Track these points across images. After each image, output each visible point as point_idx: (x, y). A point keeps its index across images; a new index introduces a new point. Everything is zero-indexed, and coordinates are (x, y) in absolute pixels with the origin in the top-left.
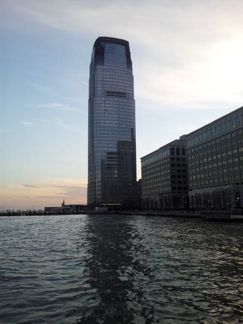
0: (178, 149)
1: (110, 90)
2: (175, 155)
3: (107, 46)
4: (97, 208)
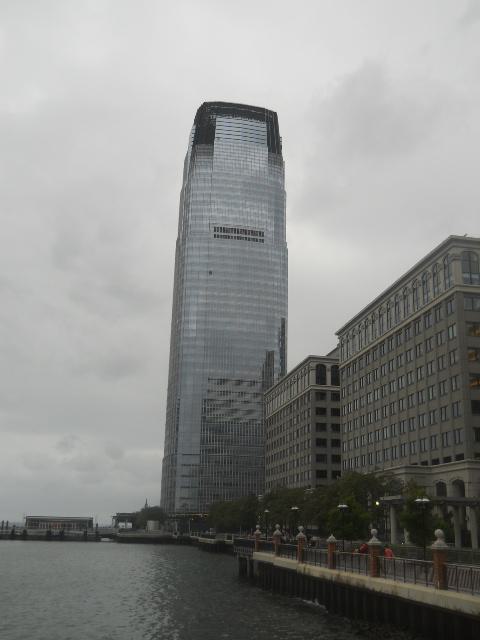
0: (335, 369)
1: (221, 224)
2: (329, 386)
3: (223, 125)
4: (151, 524)
